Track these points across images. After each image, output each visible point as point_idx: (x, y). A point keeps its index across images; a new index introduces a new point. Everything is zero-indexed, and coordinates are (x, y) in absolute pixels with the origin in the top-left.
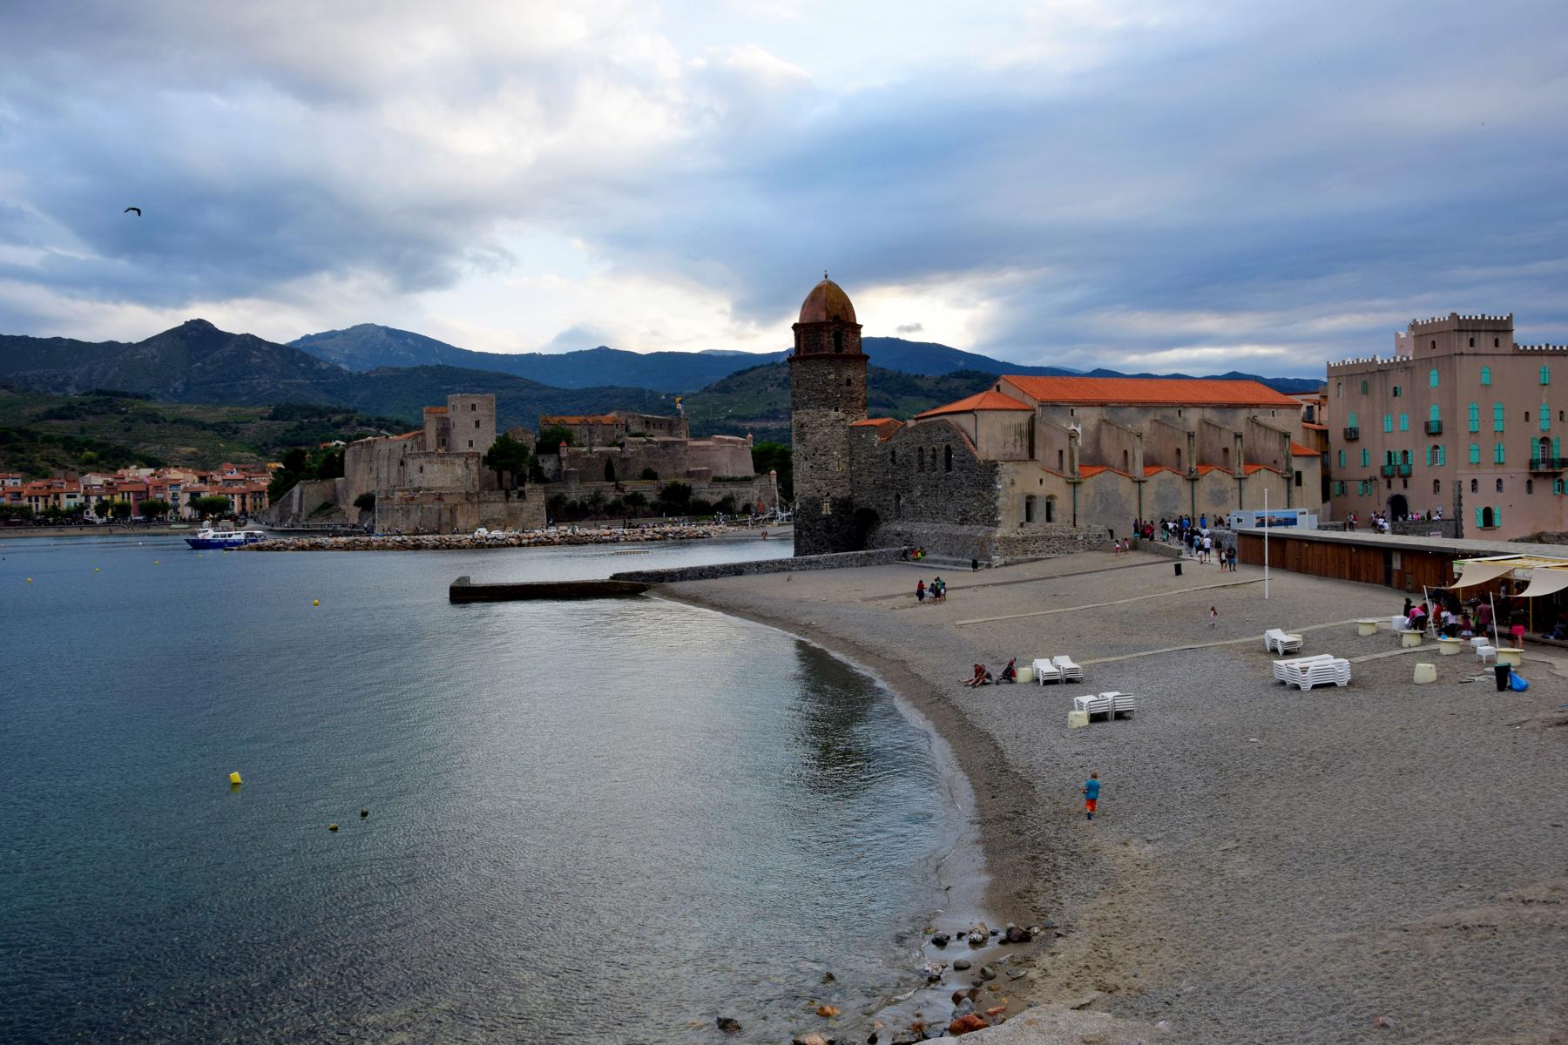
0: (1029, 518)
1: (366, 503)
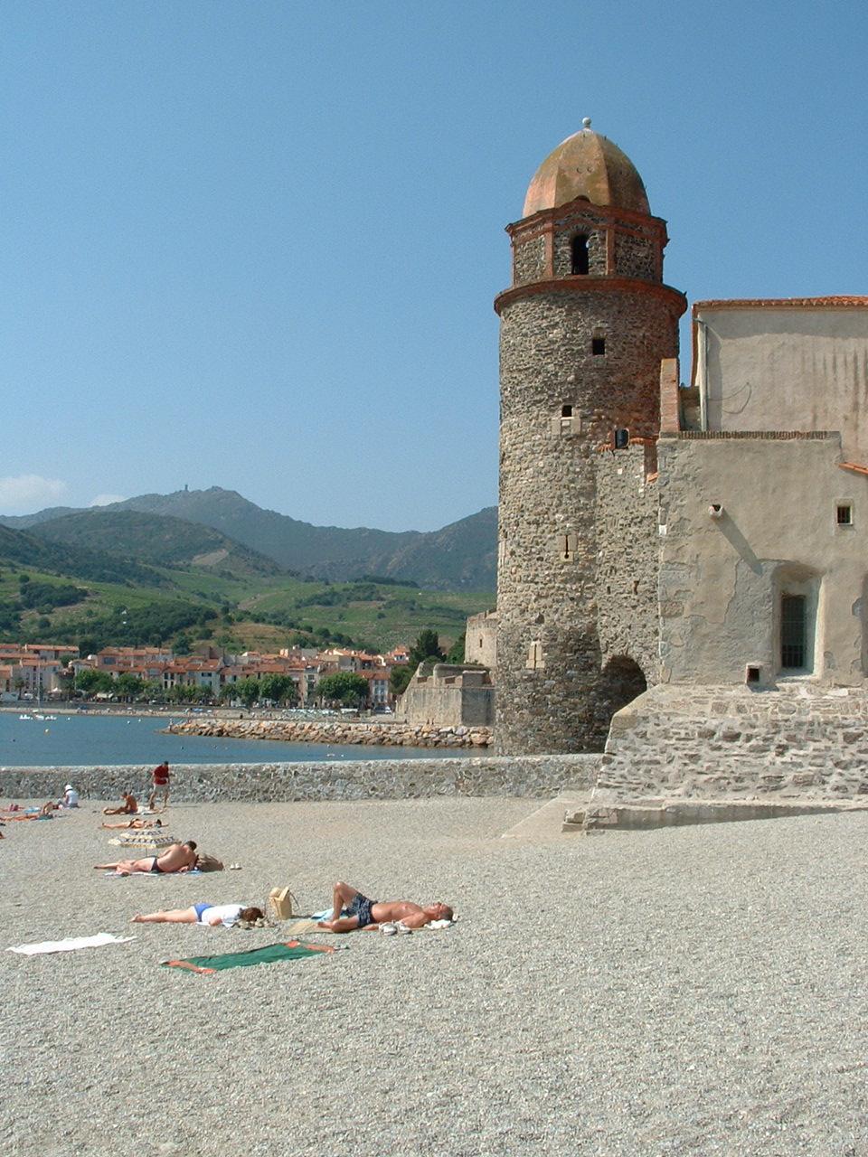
0: (793, 656)
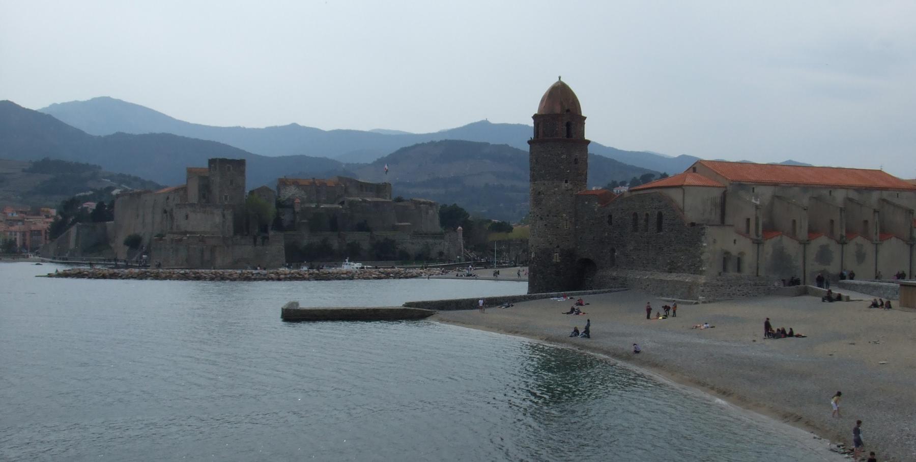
1: (134, 243)
